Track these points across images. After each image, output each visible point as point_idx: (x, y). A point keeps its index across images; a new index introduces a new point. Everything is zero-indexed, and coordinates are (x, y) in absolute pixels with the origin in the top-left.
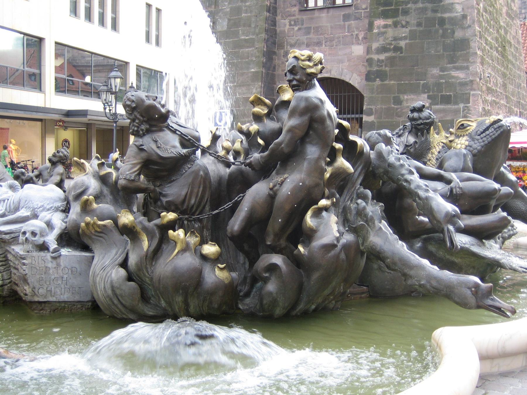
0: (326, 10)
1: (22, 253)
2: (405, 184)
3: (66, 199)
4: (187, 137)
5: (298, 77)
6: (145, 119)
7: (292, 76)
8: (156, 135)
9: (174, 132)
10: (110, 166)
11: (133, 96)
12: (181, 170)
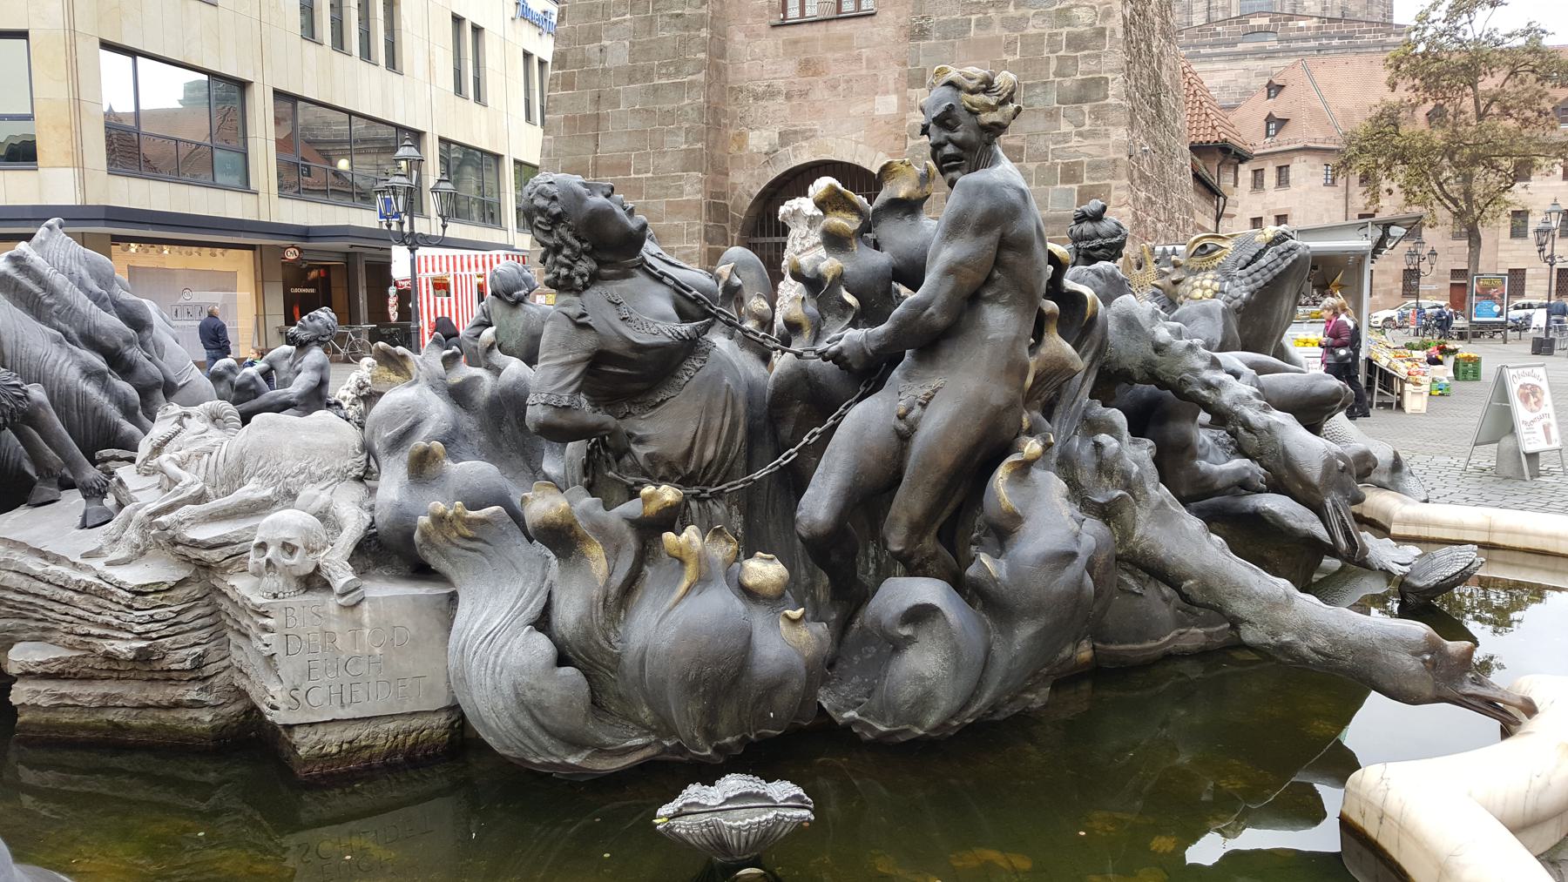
1: (257, 599)
2: (1205, 393)
3: (367, 448)
4: (690, 291)
5: (958, 135)
6: (585, 246)
7: (946, 134)
8: (616, 288)
9: (659, 278)
10: (473, 362)
11: (551, 183)
12: (679, 374)
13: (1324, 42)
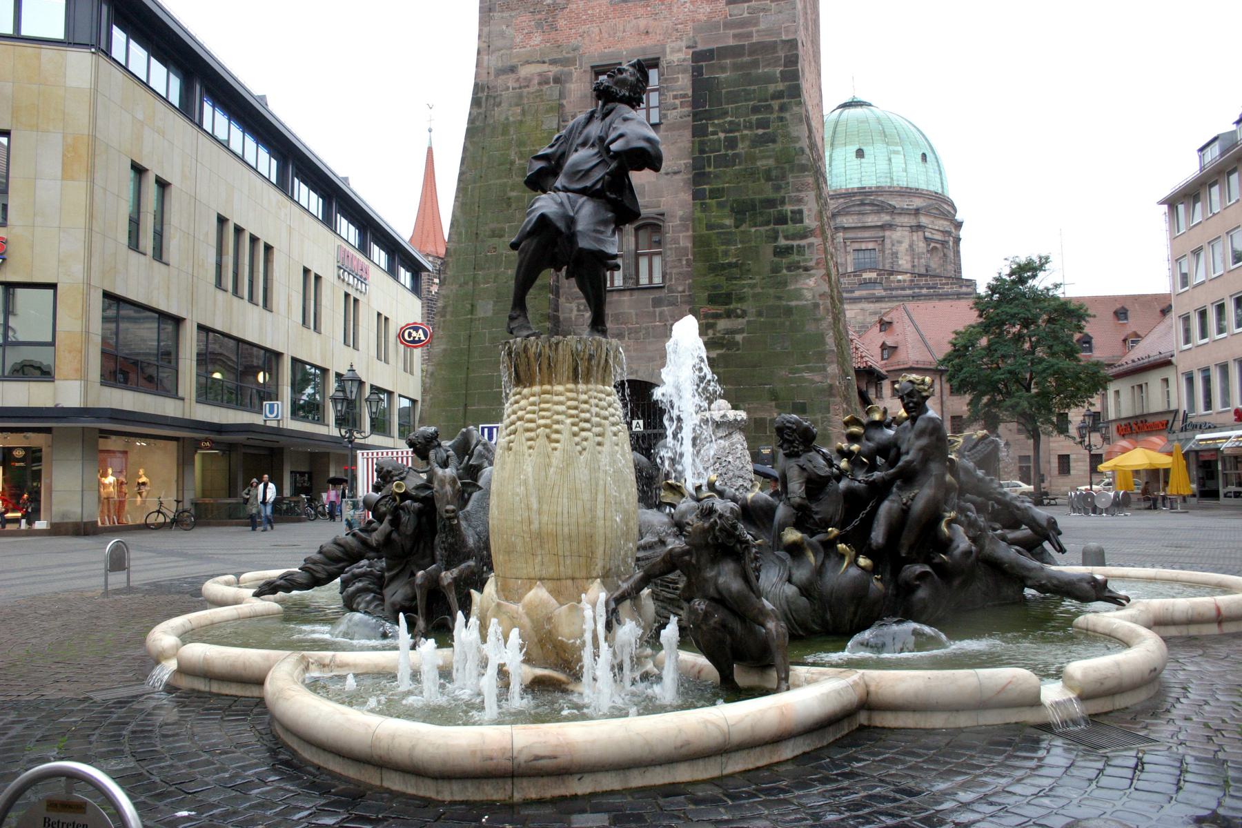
0: (628, 293)
9: (818, 452)
13: (917, 291)
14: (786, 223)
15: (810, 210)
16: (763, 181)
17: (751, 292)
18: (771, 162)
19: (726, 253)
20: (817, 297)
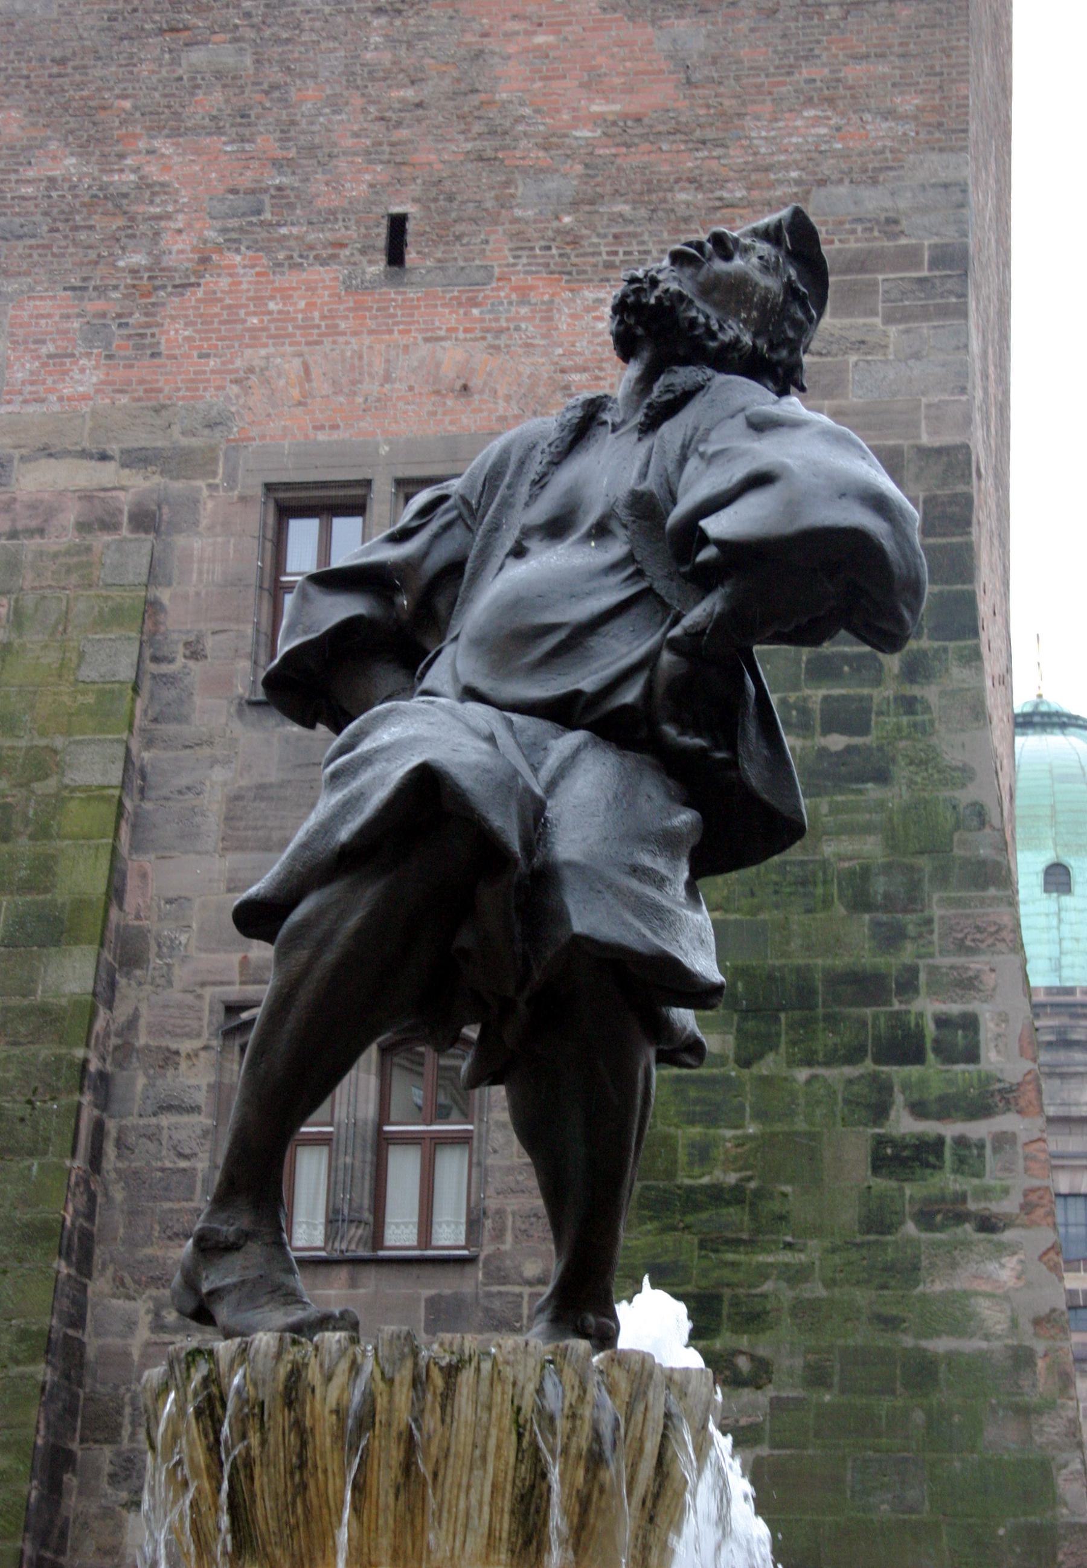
0: (343, 1274)
14: (918, 1058)
15: (1003, 1018)
16: (840, 910)
17: (788, 1295)
18: (871, 847)
19: (702, 1153)
20: (1027, 1327)
